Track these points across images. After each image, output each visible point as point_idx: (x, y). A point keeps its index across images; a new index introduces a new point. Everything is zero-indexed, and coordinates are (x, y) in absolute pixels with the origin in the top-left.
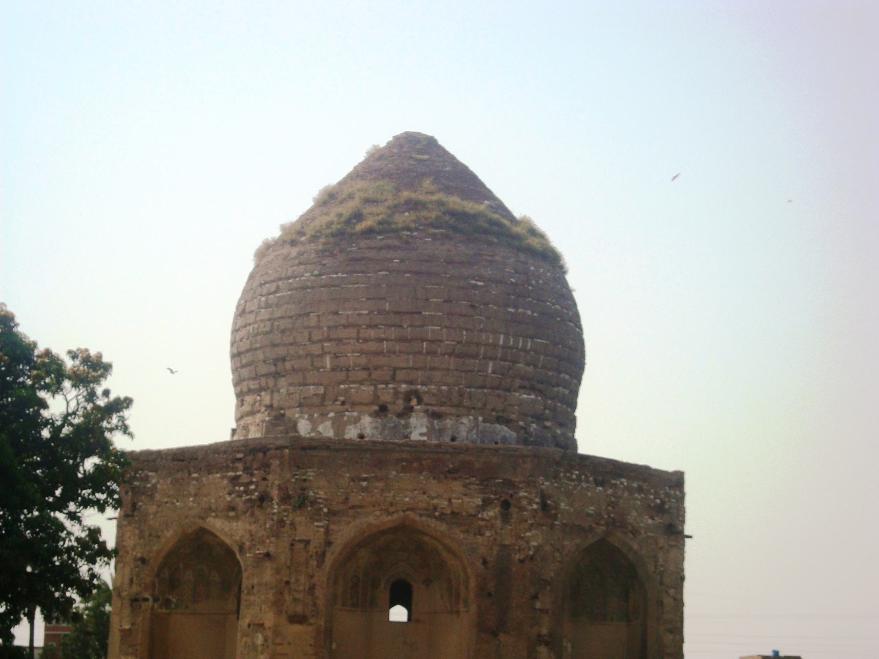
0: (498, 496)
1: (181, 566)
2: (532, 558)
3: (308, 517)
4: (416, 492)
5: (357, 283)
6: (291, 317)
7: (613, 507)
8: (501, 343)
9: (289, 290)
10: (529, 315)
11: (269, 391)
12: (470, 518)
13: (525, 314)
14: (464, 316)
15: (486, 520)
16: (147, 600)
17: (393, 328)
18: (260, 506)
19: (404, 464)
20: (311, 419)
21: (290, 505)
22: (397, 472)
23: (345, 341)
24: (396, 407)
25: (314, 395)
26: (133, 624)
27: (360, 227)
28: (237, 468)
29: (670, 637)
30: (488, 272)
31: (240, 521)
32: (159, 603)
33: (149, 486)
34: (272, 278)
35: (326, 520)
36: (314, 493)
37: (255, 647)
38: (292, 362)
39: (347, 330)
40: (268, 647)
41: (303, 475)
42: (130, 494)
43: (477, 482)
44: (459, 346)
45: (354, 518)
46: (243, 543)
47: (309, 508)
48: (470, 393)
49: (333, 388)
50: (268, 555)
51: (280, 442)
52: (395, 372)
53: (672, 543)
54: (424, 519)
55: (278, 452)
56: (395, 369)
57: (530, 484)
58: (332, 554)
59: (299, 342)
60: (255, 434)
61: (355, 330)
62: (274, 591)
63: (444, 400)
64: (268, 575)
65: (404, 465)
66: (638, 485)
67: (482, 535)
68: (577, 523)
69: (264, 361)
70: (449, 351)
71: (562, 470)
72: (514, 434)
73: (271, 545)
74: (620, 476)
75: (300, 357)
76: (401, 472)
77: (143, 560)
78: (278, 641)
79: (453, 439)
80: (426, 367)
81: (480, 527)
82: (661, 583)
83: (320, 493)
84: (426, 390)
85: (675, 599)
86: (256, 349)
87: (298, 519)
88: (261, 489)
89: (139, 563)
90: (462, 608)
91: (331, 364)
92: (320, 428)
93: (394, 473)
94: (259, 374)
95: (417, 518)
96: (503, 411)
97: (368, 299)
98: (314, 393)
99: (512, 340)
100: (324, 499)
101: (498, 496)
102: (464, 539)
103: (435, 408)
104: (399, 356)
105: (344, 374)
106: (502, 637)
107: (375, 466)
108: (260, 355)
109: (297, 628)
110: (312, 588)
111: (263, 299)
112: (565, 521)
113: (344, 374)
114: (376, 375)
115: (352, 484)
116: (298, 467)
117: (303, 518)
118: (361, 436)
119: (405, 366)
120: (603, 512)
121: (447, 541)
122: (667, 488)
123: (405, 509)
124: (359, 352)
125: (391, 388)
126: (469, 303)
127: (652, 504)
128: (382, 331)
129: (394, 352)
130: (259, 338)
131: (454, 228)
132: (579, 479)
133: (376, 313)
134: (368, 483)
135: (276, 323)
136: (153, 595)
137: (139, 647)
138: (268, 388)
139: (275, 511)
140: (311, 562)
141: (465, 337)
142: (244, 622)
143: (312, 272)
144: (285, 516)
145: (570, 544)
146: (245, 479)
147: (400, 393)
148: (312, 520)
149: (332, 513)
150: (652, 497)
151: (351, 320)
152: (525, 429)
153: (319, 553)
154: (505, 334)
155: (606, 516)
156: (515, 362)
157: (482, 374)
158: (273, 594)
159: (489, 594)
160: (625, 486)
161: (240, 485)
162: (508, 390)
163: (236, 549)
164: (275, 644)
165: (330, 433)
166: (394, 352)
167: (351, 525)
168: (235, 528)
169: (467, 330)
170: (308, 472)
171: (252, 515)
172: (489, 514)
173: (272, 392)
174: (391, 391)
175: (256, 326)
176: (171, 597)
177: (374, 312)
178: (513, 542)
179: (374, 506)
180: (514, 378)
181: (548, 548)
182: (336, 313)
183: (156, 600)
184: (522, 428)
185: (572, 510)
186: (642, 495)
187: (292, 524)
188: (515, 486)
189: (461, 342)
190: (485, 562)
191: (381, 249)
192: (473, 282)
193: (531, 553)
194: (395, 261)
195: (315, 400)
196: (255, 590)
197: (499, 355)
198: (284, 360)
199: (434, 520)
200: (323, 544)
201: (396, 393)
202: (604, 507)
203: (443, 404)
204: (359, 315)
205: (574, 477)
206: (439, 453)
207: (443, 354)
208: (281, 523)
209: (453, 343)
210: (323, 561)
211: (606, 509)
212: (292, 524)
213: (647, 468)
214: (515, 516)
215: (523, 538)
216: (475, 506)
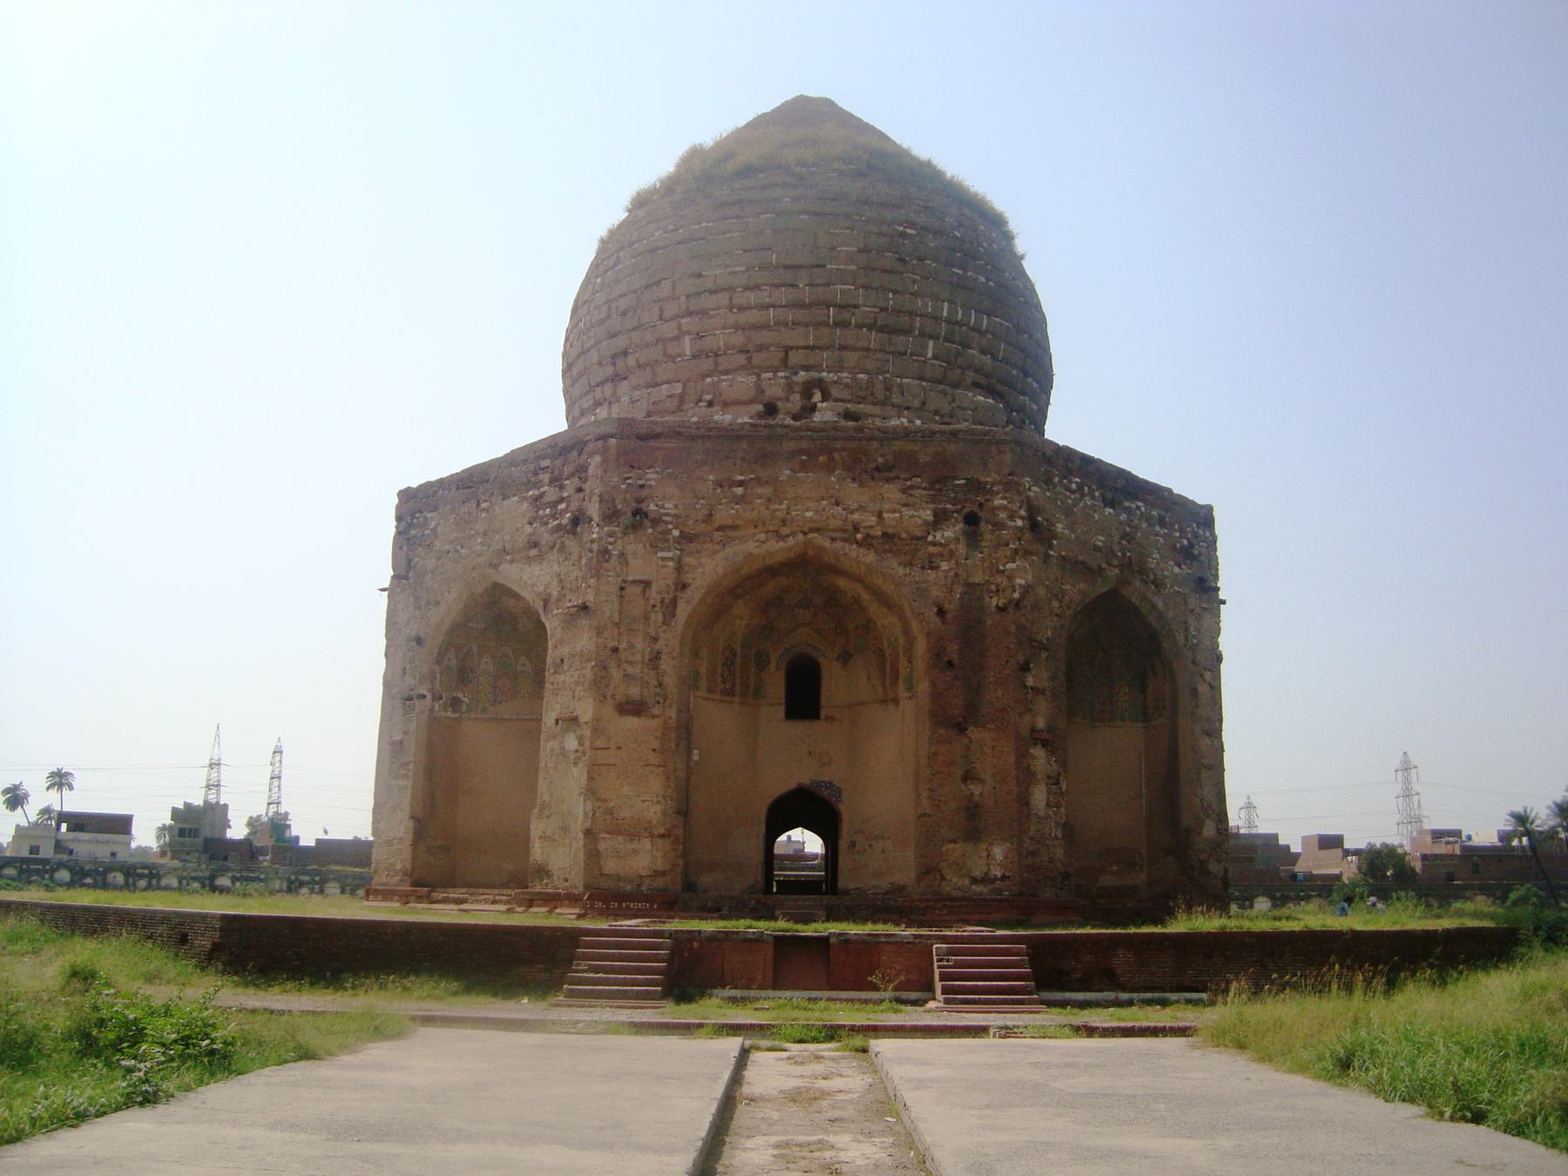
0: (959, 507)
1: (475, 650)
2: (1018, 605)
3: (648, 545)
4: (824, 502)
5: (730, 232)
6: (635, 292)
7: (1128, 541)
8: (945, 314)
9: (634, 258)
10: (982, 283)
12: (914, 542)
13: (976, 279)
14: (889, 272)
15: (941, 544)
16: (424, 697)
17: (784, 289)
18: (574, 534)
19: (804, 458)
21: (618, 526)
22: (793, 470)
23: (711, 312)
24: (789, 405)
25: (668, 397)
26: (405, 733)
27: (730, 167)
28: (542, 481)
29: (1207, 741)
31: (544, 563)
32: (441, 702)
33: (427, 532)
35: (676, 549)
36: (657, 506)
37: (563, 753)
38: (636, 355)
40: (584, 753)
41: (640, 479)
42: (405, 548)
43: (924, 485)
44: (883, 314)
45: (724, 545)
46: (550, 595)
47: (650, 531)
48: (901, 386)
49: (696, 382)
50: (584, 608)
51: (602, 430)
52: (787, 352)
53: (1204, 605)
54: (839, 544)
55: (600, 443)
56: (787, 349)
57: (1010, 486)
58: (687, 602)
59: (646, 323)
62: (593, 663)
63: (862, 394)
64: (584, 640)
65: (802, 462)
66: (1159, 515)
67: (936, 568)
68: (1081, 558)
69: (600, 364)
70: (867, 322)
71: (1057, 473)
73: (589, 590)
74: (1134, 496)
76: (799, 472)
77: (419, 641)
78: (600, 743)
80: (834, 346)
81: (931, 556)
82: (1194, 662)
83: (666, 505)
84: (835, 378)
85: (1212, 687)
87: (631, 548)
88: (574, 506)
90: (902, 692)
91: (692, 348)
93: (788, 472)
94: (593, 383)
95: (827, 544)
97: (744, 251)
98: (668, 393)
99: (960, 312)
100: (675, 515)
101: (959, 507)
102: (906, 575)
103: (849, 406)
104: (794, 329)
105: (710, 362)
106: (974, 733)
107: (755, 462)
108: (594, 356)
109: (631, 722)
110: (656, 658)
111: (599, 280)
112: (1063, 553)
113: (710, 362)
114: (758, 359)
115: (719, 490)
116: (633, 467)
117: (641, 546)
119: (802, 344)
120: (1116, 548)
121: (878, 581)
122: (1195, 525)
123: (806, 529)
124: (733, 328)
125: (782, 377)
126: (896, 256)
127: (1178, 545)
128: (766, 293)
129: (786, 324)
130: (592, 333)
132: (1080, 487)
133: (757, 269)
134: (745, 489)
135: (614, 305)
136: (431, 690)
137: (411, 766)
138: (605, 399)
139: (595, 536)
140: (653, 616)
141: (891, 302)
142: (549, 718)
143: (666, 227)
144: (611, 543)
145: (1076, 590)
146: (551, 494)
147: (797, 384)
148: (655, 548)
149: (687, 538)
150: (1178, 534)
153: (667, 601)
154: (950, 302)
155: (1119, 554)
156: (966, 346)
157: (918, 358)
158: (592, 667)
159: (950, 664)
160: (1142, 513)
162: (955, 386)
163: (539, 606)
164: (596, 749)
166: (786, 324)
167: (720, 556)
168: (537, 573)
169: (895, 292)
170: (647, 473)
171: (562, 549)
172: (946, 534)
173: (610, 403)
174: (782, 381)
175: (589, 317)
176: (460, 695)
177: (754, 268)
178: (987, 578)
179: (756, 527)
180: (965, 369)
181: (1041, 591)
182: (700, 275)
185: (1073, 536)
186: (1166, 531)
187: (622, 555)
188: (985, 488)
189: (887, 309)
190: (941, 612)
192: (901, 229)
193: (1016, 595)
194: (784, 200)
197: (943, 333)
198: (625, 353)
199: (854, 546)
200: (673, 587)
201: (790, 387)
202: (1117, 538)
203: (861, 400)
204: (730, 274)
205: (1074, 486)
206: (860, 440)
207: (860, 326)
208: (605, 553)
209: (875, 310)
210: (674, 616)
211: (1120, 543)
212: (622, 555)
213: (1169, 491)
214: (988, 536)
215: (1003, 572)
216: (920, 522)
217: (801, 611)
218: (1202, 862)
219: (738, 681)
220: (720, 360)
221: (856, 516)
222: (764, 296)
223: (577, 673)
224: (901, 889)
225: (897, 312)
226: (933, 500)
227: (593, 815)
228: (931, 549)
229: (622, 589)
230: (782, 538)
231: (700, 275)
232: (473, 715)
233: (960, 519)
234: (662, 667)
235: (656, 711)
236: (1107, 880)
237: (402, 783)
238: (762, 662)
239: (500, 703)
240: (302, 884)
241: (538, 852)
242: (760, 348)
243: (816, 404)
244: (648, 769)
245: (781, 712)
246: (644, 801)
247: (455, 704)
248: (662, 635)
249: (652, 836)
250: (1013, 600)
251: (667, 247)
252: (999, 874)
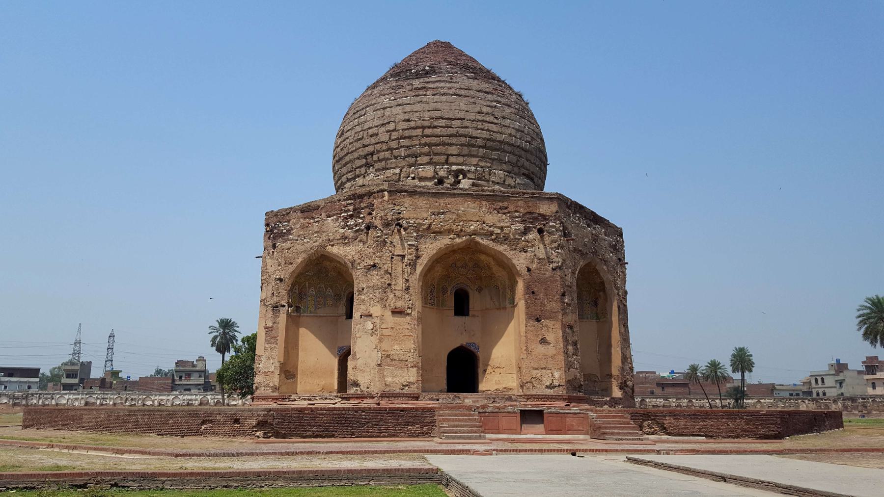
1: (307, 285)
6: (377, 126)
11: (362, 177)
16: (284, 306)
21: (390, 230)
26: (274, 323)
30: (503, 100)
34: (361, 108)
37: (365, 331)
39: (416, 131)
50: (374, 266)
52: (448, 157)
55: (380, 194)
56: (448, 155)
61: (421, 130)
70: (481, 144)
75: (383, 151)
77: (281, 280)
89: (278, 282)
100: (416, 227)
110: (407, 289)
116: (395, 204)
123: (471, 234)
125: (446, 168)
142: (356, 315)
144: (387, 238)
147: (452, 171)
168: (348, 251)
173: (364, 177)
176: (300, 305)
182: (408, 120)
183: (290, 306)
196: (364, 292)
198: (372, 154)
199: (491, 242)
201: (450, 172)
203: (479, 179)
207: (479, 147)
217: (463, 269)
219: (436, 299)
220: (418, 159)
221: (491, 229)
222: (438, 131)
223: (371, 295)
226: (523, 222)
227: (381, 358)
229: (392, 258)
230: (459, 236)
231: (408, 120)
232: (305, 315)
233: (536, 231)
234: (411, 293)
235: (409, 311)
237: (272, 346)
238: (444, 291)
239: (318, 309)
243: (460, 180)
244: (406, 337)
245: (453, 312)
246: (404, 352)
248: (410, 279)
250: (557, 267)
251: (392, 107)
252: (556, 383)
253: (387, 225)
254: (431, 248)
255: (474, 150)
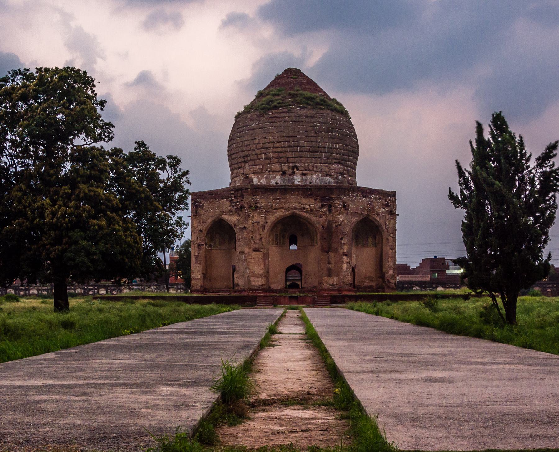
2: (340, 225)
6: (249, 140)
13: (335, 135)
14: (313, 137)
16: (203, 245)
18: (241, 211)
20: (258, 178)
30: (321, 120)
48: (316, 166)
50: (244, 228)
56: (288, 158)
60: (238, 184)
67: (322, 217)
72: (333, 180)
75: (253, 155)
77: (201, 231)
78: (250, 257)
79: (310, 183)
81: (321, 215)
82: (388, 232)
86: (237, 153)
87: (255, 215)
90: (315, 244)
92: (261, 181)
96: (329, 172)
106: (330, 254)
110: (261, 239)
118: (276, 183)
119: (291, 156)
131: (308, 104)
132: (357, 195)
136: (205, 243)
145: (355, 220)
146: (235, 200)
148: (260, 214)
151: (271, 140)
152: (337, 178)
156: (332, 153)
161: (233, 203)
162: (330, 164)
163: (233, 226)
165: (265, 183)
166: (287, 152)
176: (211, 244)
181: (346, 221)
182: (265, 138)
183: (206, 245)
184: (336, 178)
190: (323, 227)
191: (281, 113)
193: (340, 223)
195: (259, 171)
198: (247, 156)
201: (289, 167)
203: (306, 170)
204: (274, 138)
212: (253, 216)
213: (382, 190)
214: (333, 210)
218: (388, 280)
222: (282, 144)
224: (315, 287)
225: (314, 147)
226: (321, 202)
228: (322, 213)
230: (288, 211)
235: (262, 250)
236: (366, 284)
237: (199, 265)
238: (284, 237)
240: (90, 290)
241: (236, 281)
242: (281, 158)
247: (210, 246)
249: (261, 277)
253: (250, 207)
254: (272, 218)
255: (303, 154)
